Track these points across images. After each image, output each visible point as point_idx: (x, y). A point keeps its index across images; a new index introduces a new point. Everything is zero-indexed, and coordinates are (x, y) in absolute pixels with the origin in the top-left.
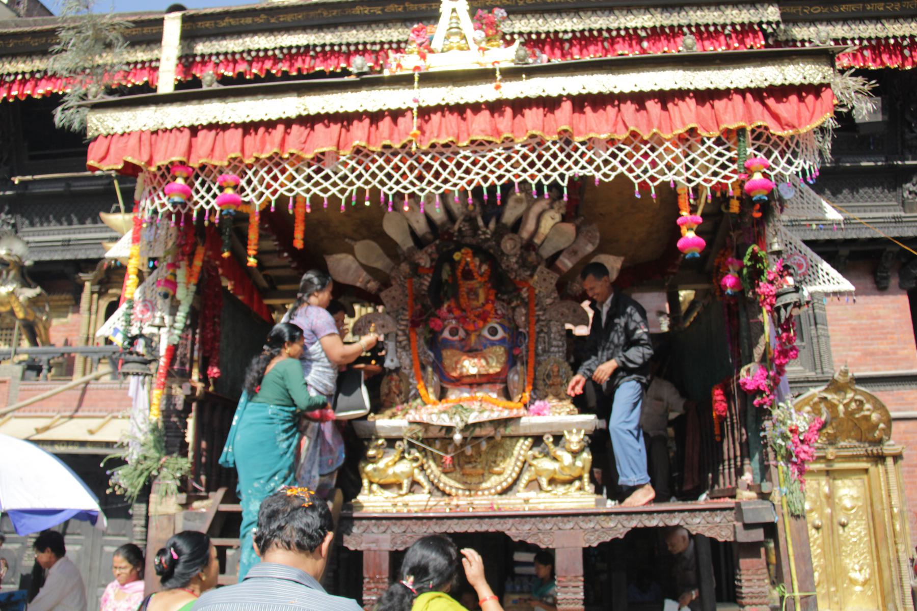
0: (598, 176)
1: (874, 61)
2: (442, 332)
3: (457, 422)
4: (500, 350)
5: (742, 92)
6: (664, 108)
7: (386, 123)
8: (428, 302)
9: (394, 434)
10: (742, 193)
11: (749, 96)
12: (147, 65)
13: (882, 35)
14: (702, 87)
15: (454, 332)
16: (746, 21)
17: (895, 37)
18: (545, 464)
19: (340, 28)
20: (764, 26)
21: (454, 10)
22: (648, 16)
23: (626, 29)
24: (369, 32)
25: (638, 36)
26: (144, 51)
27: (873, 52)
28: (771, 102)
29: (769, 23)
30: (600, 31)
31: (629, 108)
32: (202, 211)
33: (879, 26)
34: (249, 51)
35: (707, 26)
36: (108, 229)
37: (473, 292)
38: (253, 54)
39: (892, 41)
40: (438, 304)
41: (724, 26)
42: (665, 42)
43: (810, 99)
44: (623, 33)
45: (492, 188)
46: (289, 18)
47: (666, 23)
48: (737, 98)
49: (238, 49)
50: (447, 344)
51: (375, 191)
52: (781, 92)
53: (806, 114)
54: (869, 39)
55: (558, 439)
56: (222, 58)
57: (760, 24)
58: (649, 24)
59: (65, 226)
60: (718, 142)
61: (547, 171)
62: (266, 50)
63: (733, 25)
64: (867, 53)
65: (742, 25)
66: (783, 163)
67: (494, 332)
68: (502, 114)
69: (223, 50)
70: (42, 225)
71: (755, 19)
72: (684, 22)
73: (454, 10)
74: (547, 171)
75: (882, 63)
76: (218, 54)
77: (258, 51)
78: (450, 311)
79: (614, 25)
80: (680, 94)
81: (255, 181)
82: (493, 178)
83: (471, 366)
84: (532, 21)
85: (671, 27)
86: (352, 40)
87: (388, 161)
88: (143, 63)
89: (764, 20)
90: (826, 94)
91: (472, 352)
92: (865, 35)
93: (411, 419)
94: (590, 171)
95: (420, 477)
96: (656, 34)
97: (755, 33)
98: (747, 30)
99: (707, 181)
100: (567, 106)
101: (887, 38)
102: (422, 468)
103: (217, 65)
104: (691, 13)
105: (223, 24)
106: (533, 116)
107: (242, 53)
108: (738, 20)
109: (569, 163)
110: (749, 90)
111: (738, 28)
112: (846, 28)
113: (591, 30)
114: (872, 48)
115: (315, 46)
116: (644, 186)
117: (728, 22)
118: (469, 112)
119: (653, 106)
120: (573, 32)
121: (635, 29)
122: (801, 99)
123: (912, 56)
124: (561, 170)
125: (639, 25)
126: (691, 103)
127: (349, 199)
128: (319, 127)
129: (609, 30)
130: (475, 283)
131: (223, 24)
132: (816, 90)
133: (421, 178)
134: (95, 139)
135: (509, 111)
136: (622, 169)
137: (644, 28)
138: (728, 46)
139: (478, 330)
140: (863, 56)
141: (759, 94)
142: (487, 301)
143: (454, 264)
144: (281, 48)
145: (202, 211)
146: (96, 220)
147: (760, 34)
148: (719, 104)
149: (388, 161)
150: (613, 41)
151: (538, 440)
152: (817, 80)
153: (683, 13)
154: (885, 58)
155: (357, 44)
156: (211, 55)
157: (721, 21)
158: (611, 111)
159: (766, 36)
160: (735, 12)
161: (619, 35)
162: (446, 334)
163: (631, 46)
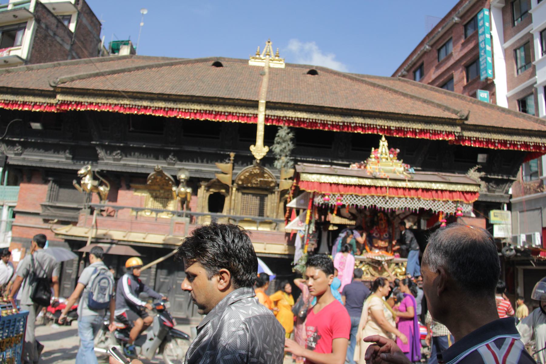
0: (425, 208)
1: (486, 146)
2: (374, 233)
3: (383, 259)
4: (388, 240)
5: (459, 192)
6: (442, 193)
7: (379, 189)
8: (369, 224)
9: (362, 260)
10: (455, 213)
11: (461, 193)
12: (246, 115)
13: (490, 138)
14: (451, 189)
15: (376, 234)
16: (450, 131)
17: (494, 139)
18: (399, 270)
19: (319, 114)
20: (455, 134)
21: (383, 145)
22: (420, 125)
23: (413, 129)
24: (328, 116)
25: (415, 131)
26: (245, 109)
27: (486, 143)
28: (465, 194)
29: (457, 132)
30: (404, 128)
31: (434, 192)
32: (332, 205)
33: (490, 134)
34: (286, 117)
35: (438, 131)
36: (315, 210)
37: (382, 225)
38: (288, 118)
39: (493, 141)
40: (373, 227)
41: (443, 131)
42: (423, 135)
43: (473, 195)
44: (411, 130)
45: (402, 208)
46: (302, 108)
47: (426, 128)
48: (458, 193)
49: (282, 115)
50: (374, 237)
51: (375, 206)
52: (467, 192)
53: (472, 198)
54: (486, 139)
55: (402, 264)
56: (276, 118)
57: (454, 132)
58: (420, 128)
59: (195, 164)
60: (452, 202)
61: (414, 205)
62: (292, 118)
63: (446, 132)
64: (485, 143)
65: (449, 132)
66: (465, 208)
67: (386, 235)
68: (406, 190)
69: (276, 115)
70: (185, 161)
71: (453, 131)
72: (431, 128)
73: (383, 145)
74: (414, 205)
75: (488, 146)
76: (274, 116)
77: (289, 117)
78: (376, 229)
79: (409, 127)
80: (446, 190)
81: (346, 199)
82: (402, 206)
83: (382, 244)
84: (383, 121)
85: (427, 130)
86: (323, 119)
87: (378, 198)
88: (245, 114)
89: (456, 131)
90: (477, 194)
91: (382, 240)
92: (485, 137)
93: (368, 257)
94: (424, 207)
95: (368, 271)
96: (422, 131)
97: (452, 135)
98: (449, 134)
99: (449, 212)
100: (420, 190)
101: (491, 139)
102: (368, 269)
103: (273, 120)
104: (433, 126)
105: (277, 105)
106: (413, 192)
107: (283, 117)
108: (448, 130)
109: (419, 204)
110: (461, 191)
111: (447, 133)
112: (480, 134)
113: (401, 128)
114: (486, 142)
115: (310, 119)
116: (435, 211)
117: (444, 130)
118: (398, 189)
119: (439, 192)
120: (396, 127)
121: (415, 129)
122: (471, 195)
123: (498, 147)
124: (417, 206)
125: (417, 128)
126: (448, 193)
127: (369, 207)
128: (362, 188)
129: (407, 128)
130: (382, 222)
131: (277, 105)
132: (474, 193)
133: (386, 203)
134: (303, 181)
135: (407, 190)
136: (431, 207)
137: (418, 129)
138: (443, 138)
139: (383, 235)
140: (483, 144)
141: (463, 192)
142: (385, 227)
143: (378, 217)
144: (298, 118)
145: (332, 205)
146: (215, 164)
147: (454, 135)
148: (454, 194)
149: (378, 198)
150: (407, 132)
151: (397, 264)
152: (476, 190)
153: (431, 125)
154: (490, 145)
155: (324, 121)
156: (272, 116)
157: (442, 130)
158: (430, 193)
159: (455, 136)
160: (447, 127)
161: (410, 131)
162: (374, 235)
163: (412, 135)
